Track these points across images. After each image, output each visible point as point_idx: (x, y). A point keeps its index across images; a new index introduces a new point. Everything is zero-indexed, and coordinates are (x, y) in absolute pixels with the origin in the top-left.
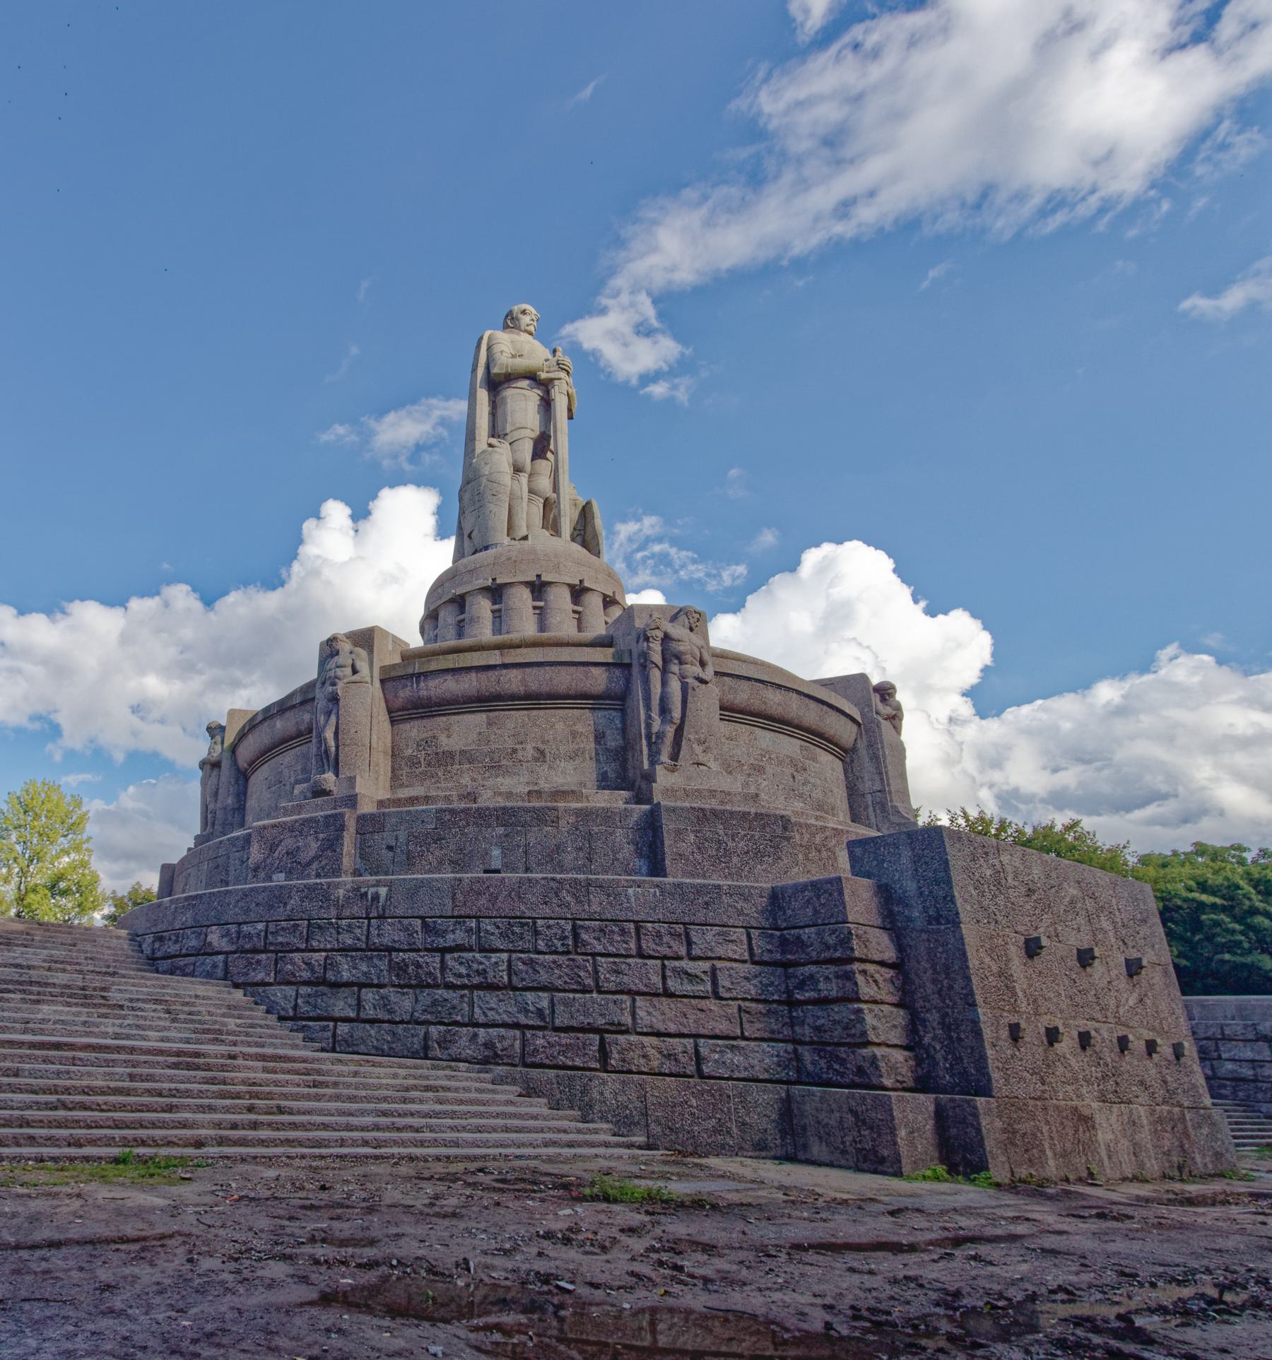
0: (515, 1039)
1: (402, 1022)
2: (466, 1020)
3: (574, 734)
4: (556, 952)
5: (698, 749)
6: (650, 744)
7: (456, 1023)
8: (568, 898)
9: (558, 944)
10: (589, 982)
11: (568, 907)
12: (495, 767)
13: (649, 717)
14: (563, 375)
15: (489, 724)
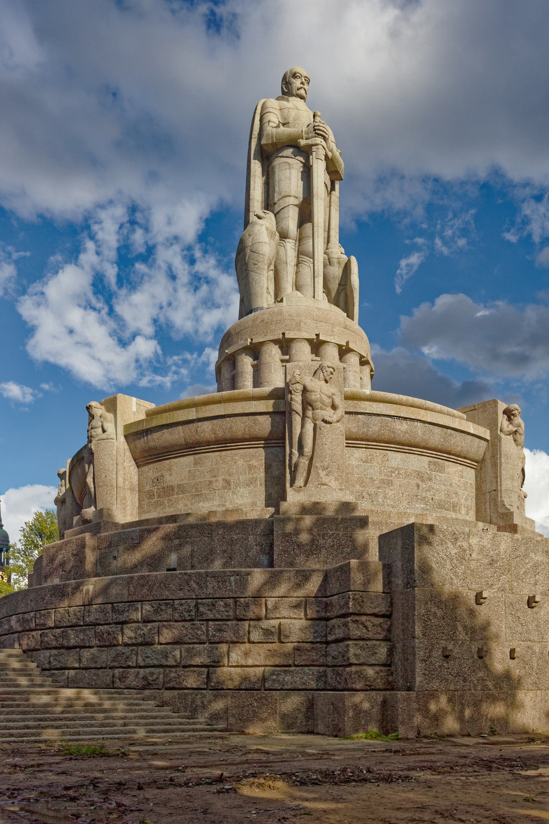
0: (160, 674)
1: (101, 668)
2: (134, 665)
3: (250, 467)
4: (185, 620)
5: (322, 473)
6: (290, 473)
7: (129, 667)
8: (194, 586)
9: (187, 615)
10: (204, 638)
11: (194, 591)
12: (198, 496)
13: (291, 453)
14: (319, 140)
15: (195, 464)
